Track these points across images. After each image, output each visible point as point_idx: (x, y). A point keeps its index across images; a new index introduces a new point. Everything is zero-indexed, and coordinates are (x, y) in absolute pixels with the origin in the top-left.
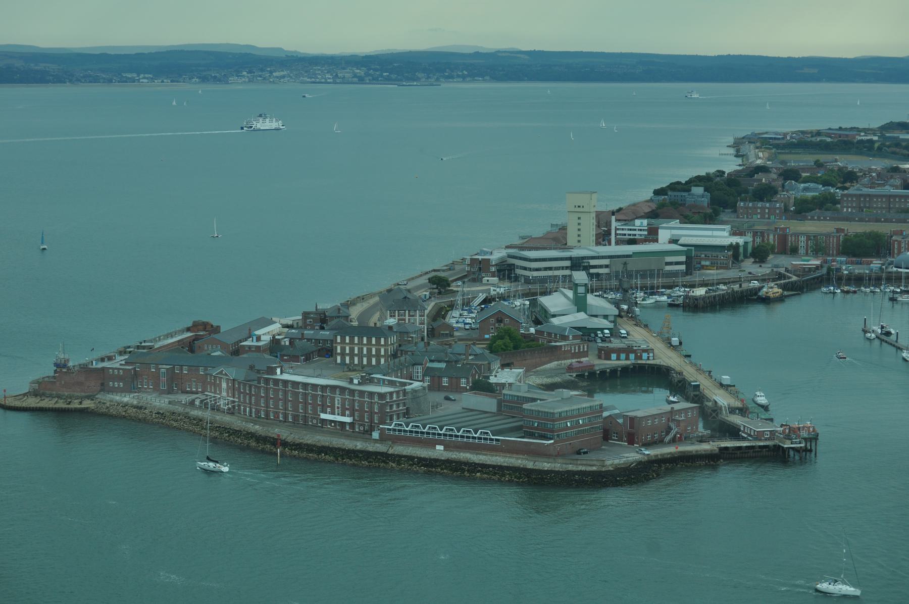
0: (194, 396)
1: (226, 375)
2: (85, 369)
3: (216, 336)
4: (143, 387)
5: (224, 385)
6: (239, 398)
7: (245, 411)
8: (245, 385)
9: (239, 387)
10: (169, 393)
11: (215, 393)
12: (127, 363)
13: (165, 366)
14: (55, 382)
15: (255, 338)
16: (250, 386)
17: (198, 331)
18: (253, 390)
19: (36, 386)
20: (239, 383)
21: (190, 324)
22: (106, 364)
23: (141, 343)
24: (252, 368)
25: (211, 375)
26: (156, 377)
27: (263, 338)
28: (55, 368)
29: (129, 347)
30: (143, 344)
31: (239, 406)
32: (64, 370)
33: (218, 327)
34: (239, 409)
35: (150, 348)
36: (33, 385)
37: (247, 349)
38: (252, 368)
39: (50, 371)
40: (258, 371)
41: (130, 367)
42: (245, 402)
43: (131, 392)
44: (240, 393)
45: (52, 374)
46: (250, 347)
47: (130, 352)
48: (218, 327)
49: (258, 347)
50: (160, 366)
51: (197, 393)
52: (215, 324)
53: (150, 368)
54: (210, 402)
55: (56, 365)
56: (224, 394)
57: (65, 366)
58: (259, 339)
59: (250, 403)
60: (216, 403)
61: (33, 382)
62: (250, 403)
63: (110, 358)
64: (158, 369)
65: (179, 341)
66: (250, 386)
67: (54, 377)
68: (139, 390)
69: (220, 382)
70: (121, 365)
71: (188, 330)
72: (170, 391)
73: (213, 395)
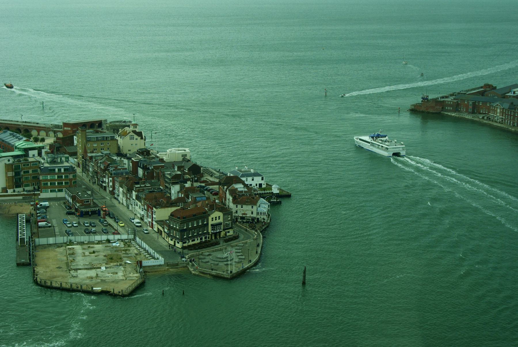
0: (485, 115)
1: (500, 106)
2: (435, 100)
3: (494, 91)
4: (461, 110)
5: (498, 111)
6: (505, 117)
7: (507, 122)
8: (508, 111)
9: (506, 111)
10: (472, 113)
11: (494, 114)
12: (454, 99)
13: (471, 101)
14: (422, 106)
15: (512, 92)
16: (511, 112)
17: (487, 88)
18: (512, 113)
19: (413, 107)
20: (506, 110)
21: (482, 85)
22: (443, 99)
23: (460, 92)
24: (512, 103)
25: (493, 106)
26: (467, 106)
27: (516, 92)
28: (422, 100)
29: (455, 93)
30: (461, 92)
31: (505, 120)
32: (426, 101)
33: (496, 87)
34: (505, 122)
35: (465, 94)
36: (412, 107)
37: (509, 97)
38: (512, 103)
39: (420, 100)
40: (515, 105)
41: (456, 101)
42: (508, 119)
43: (455, 112)
44: (506, 114)
45: (421, 102)
46: (510, 96)
47: (455, 95)
48: (496, 87)
49: (513, 97)
50: (469, 101)
51: (485, 114)
52: (494, 86)
53: (465, 102)
54: (492, 118)
55: (423, 98)
56: (498, 114)
57: (427, 99)
58: (514, 93)
59: (510, 119)
60: (494, 118)
61: (412, 105)
62: (510, 119)
63: (446, 97)
64: (468, 102)
65: (477, 92)
66: (511, 112)
67: (421, 104)
68: (459, 111)
69: (497, 109)
70: (452, 100)
71: (482, 87)
72: (473, 112)
73: (493, 115)
